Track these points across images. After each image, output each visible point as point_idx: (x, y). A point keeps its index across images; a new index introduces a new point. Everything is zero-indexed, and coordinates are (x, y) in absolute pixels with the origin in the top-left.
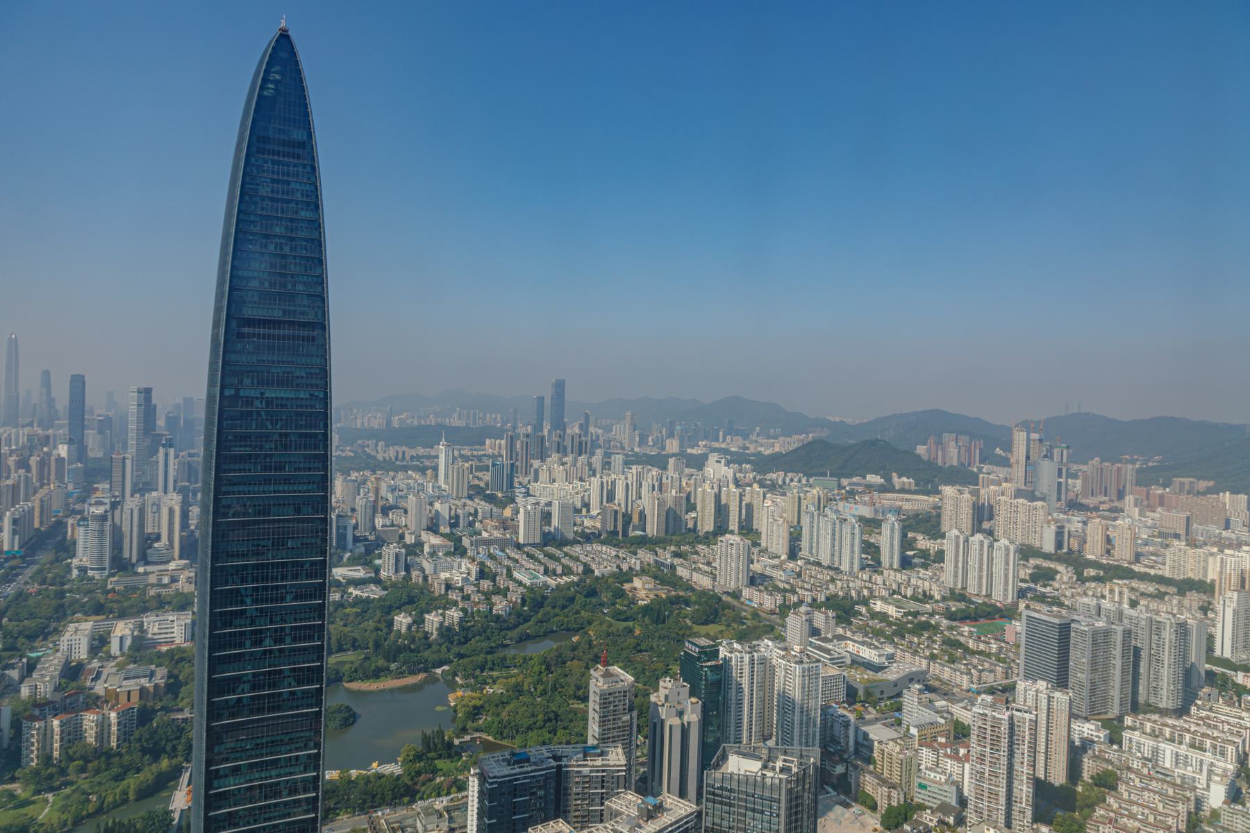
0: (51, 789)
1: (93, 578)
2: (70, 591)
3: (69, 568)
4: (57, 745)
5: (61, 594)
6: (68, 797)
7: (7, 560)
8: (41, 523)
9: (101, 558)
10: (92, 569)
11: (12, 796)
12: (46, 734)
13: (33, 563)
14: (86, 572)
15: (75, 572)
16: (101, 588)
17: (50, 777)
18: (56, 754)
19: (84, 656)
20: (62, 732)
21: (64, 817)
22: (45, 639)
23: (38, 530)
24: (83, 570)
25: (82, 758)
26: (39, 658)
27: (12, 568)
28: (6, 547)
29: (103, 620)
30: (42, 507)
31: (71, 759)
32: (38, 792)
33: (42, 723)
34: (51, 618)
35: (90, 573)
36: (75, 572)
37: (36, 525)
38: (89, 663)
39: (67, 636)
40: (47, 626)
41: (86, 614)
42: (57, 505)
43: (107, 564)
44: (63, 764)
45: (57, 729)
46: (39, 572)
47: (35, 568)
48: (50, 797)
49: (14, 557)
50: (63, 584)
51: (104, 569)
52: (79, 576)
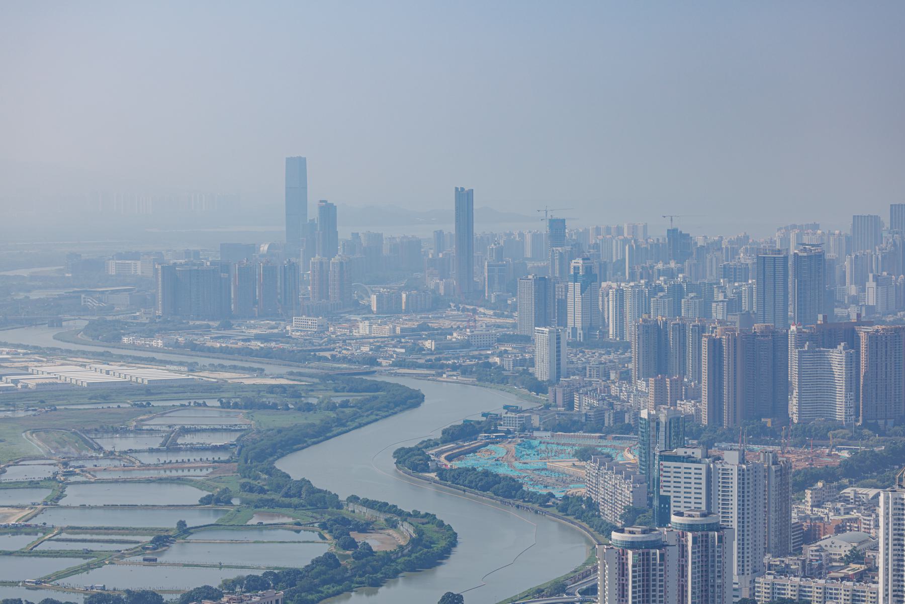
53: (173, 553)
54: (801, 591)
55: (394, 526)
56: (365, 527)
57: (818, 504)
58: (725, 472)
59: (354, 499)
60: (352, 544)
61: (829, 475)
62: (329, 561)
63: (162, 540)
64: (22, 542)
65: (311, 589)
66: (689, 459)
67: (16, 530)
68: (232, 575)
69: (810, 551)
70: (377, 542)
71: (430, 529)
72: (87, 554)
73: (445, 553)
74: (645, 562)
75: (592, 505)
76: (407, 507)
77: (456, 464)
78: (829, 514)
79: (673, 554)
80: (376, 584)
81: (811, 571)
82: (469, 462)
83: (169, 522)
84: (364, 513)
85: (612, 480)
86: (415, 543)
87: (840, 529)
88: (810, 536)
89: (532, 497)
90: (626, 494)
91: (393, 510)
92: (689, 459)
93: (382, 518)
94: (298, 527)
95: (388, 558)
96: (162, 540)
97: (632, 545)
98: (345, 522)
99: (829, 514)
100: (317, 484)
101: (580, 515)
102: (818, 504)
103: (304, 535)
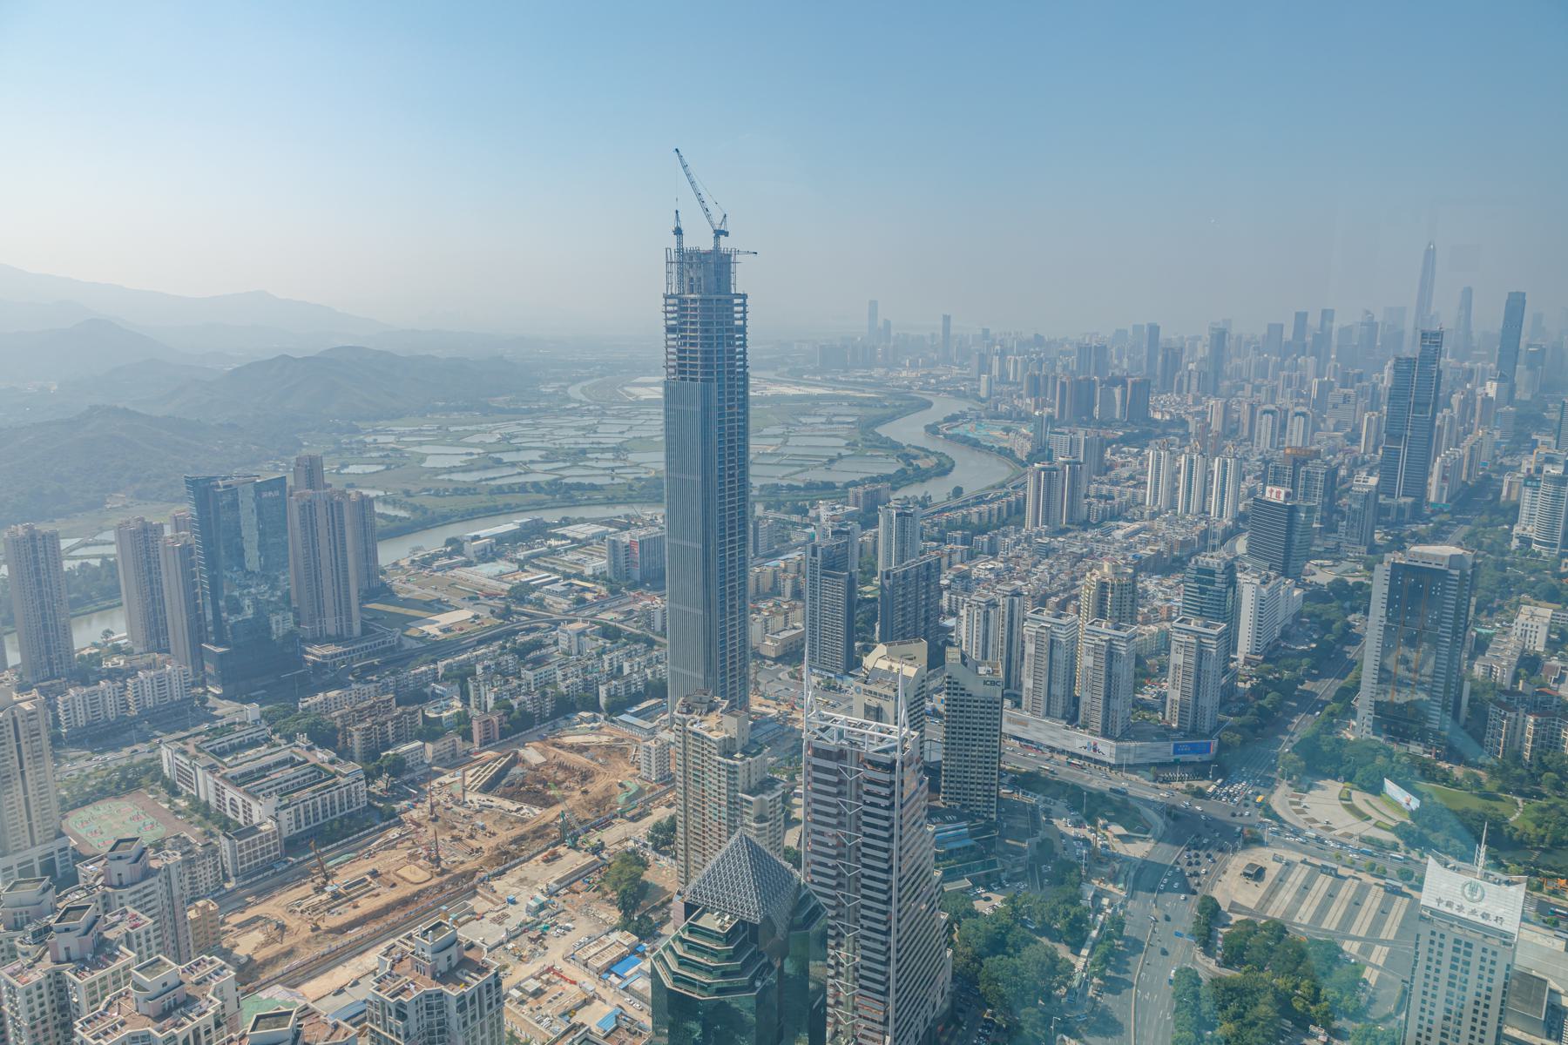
0: (1520, 793)
1: (1539, 554)
2: (1512, 565)
3: (1508, 536)
4: (1529, 745)
5: (1501, 566)
6: (1542, 810)
7: (1434, 513)
8: (1469, 475)
9: (1551, 531)
10: (1538, 543)
11: (1478, 783)
12: (1516, 729)
13: (1468, 522)
14: (1530, 546)
15: (1515, 543)
16: (1552, 569)
17: (1520, 779)
18: (1527, 755)
19: (1542, 649)
20: (1536, 732)
21: (1541, 831)
22: (1490, 614)
23: (1464, 483)
24: (1526, 541)
25: (1558, 771)
26: (1489, 637)
27: (1442, 524)
28: (1432, 499)
29: (1559, 610)
30: (1471, 456)
31: (1545, 767)
32: (1502, 789)
33: (1513, 715)
34: (1494, 592)
35: (1535, 547)
36: (1515, 543)
37: (1464, 477)
38: (1548, 659)
39: (1521, 618)
40: (1491, 601)
41: (1535, 596)
42: (1485, 454)
43: (1559, 541)
44: (1533, 770)
45: (1530, 727)
46: (1472, 534)
47: (1467, 528)
48: (1519, 800)
49: (1441, 511)
50: (1503, 554)
51: (1555, 545)
52: (1520, 548)
53: (836, 466)
54: (1110, 491)
55: (927, 457)
56: (915, 458)
57: (1113, 454)
58: (1078, 440)
59: (909, 445)
60: (912, 464)
61: (1115, 441)
62: (903, 471)
63: (832, 461)
64: (775, 460)
65: (897, 483)
66: (1063, 433)
67: (771, 454)
68: (864, 476)
69: (1112, 474)
70: (923, 464)
71: (943, 459)
72: (801, 466)
73: (951, 470)
74: (1049, 477)
75: (1012, 451)
76: (932, 450)
77: (950, 432)
78: (1117, 458)
79: (1061, 473)
80: (923, 481)
81: (1115, 483)
82: (956, 431)
83: (834, 453)
84: (915, 452)
85: (1021, 440)
86: (939, 465)
87: (1123, 465)
88: (1111, 468)
89: (986, 447)
90: (1028, 447)
91: (927, 450)
92: (1063, 433)
93: (922, 454)
94: (887, 457)
95: (927, 471)
96: (832, 461)
97: (1043, 469)
98: (907, 455)
99: (1117, 458)
100: (894, 438)
101: (1007, 455)
102: (1113, 454)
103: (890, 460)
